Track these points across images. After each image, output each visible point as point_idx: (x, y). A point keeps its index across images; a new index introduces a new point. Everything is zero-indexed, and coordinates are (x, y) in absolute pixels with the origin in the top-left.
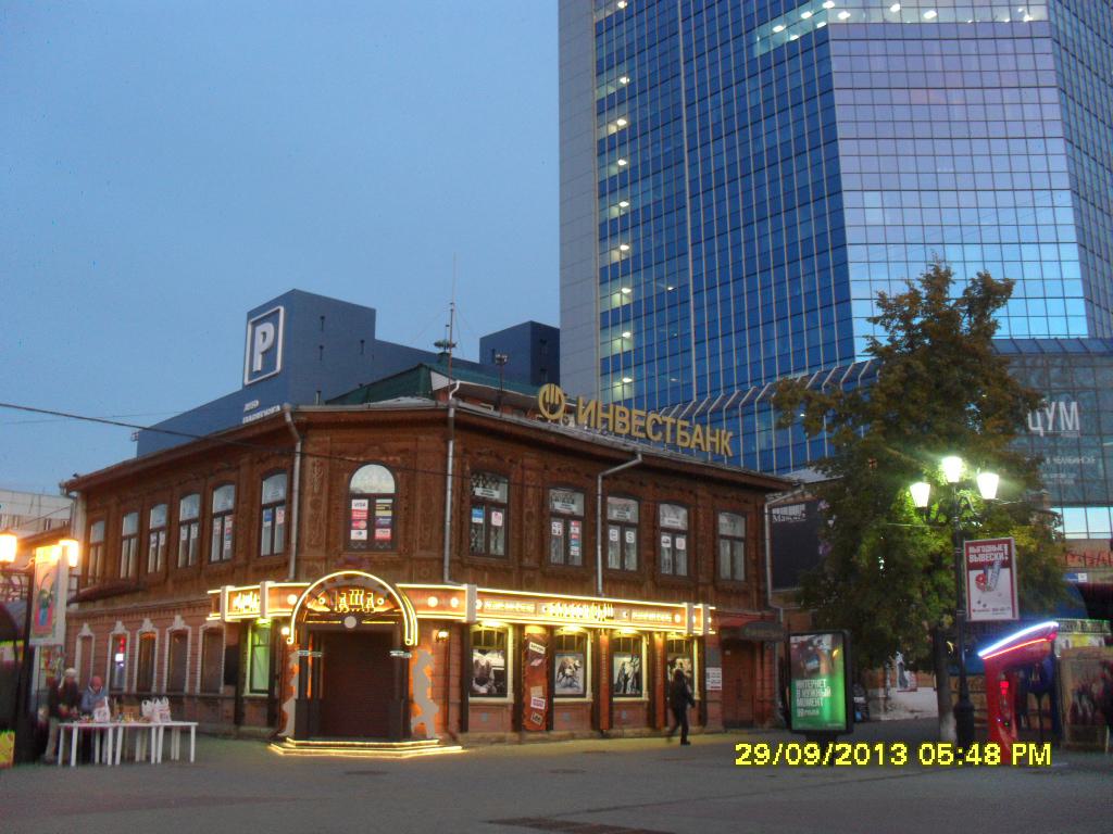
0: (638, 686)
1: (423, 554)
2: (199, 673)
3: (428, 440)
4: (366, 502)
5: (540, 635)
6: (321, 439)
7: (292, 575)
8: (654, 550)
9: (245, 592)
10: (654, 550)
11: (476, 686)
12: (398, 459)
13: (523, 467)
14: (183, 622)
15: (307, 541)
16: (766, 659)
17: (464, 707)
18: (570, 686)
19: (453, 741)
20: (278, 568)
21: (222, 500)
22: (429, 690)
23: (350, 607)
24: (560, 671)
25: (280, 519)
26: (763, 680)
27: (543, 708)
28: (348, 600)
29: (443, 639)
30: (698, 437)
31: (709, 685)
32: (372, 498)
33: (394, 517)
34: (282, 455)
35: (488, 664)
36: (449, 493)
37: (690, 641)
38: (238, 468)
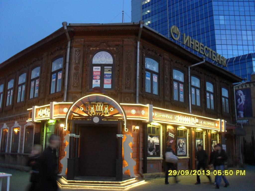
1: (127, 91)
2: (23, 146)
3: (128, 41)
4: (100, 67)
5: (172, 129)
6: (79, 40)
7: (65, 100)
9: (43, 108)
11: (149, 152)
12: (115, 49)
13: (164, 59)
14: (18, 124)
15: (72, 84)
16: (237, 142)
17: (145, 162)
18: (182, 151)
19: (140, 178)
20: (58, 98)
21: (35, 73)
22: (131, 154)
23: (96, 112)
24: (178, 145)
25: (60, 76)
26: (236, 150)
28: (95, 108)
29: (137, 130)
30: (218, 58)
32: (102, 66)
33: (112, 74)
34: (61, 49)
35: (153, 142)
36: (138, 64)
37: (216, 134)
38: (42, 59)
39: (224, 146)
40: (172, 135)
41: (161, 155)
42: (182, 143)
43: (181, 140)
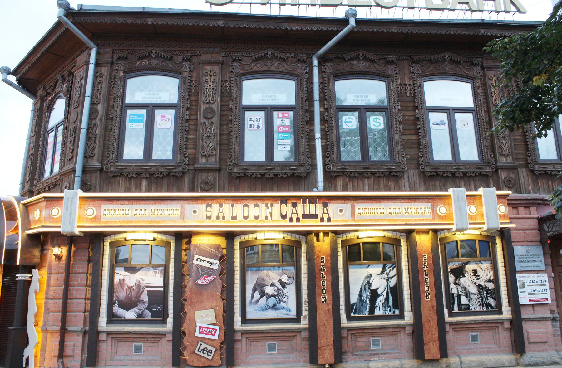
0: (398, 304)
5: (211, 246)
8: (417, 133)
10: (417, 133)
18: (274, 307)
24: (255, 290)
27: (216, 337)
31: (524, 298)
35: (139, 286)
40: (208, 262)
41: (170, 320)
42: (277, 284)
43: (267, 275)
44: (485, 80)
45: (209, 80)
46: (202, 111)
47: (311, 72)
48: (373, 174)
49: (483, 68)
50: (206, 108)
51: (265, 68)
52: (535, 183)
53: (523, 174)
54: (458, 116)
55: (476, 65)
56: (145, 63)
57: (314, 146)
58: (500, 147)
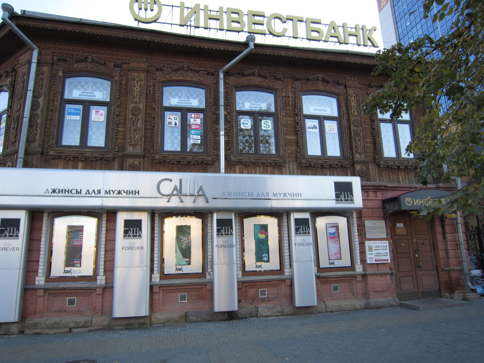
8: (297, 134)
10: (297, 134)
16: (447, 228)
26: (446, 250)
31: (371, 258)
39: (385, 245)
44: (347, 96)
45: (136, 84)
46: (130, 109)
47: (217, 83)
48: (263, 164)
49: (345, 87)
50: (134, 107)
51: (181, 78)
52: (380, 174)
53: (372, 168)
54: (327, 124)
55: (341, 84)
56: (82, 66)
57: (219, 141)
58: (356, 147)
